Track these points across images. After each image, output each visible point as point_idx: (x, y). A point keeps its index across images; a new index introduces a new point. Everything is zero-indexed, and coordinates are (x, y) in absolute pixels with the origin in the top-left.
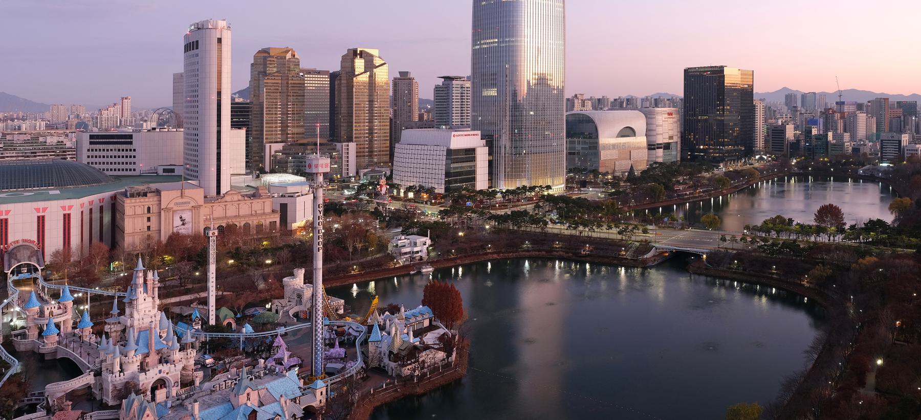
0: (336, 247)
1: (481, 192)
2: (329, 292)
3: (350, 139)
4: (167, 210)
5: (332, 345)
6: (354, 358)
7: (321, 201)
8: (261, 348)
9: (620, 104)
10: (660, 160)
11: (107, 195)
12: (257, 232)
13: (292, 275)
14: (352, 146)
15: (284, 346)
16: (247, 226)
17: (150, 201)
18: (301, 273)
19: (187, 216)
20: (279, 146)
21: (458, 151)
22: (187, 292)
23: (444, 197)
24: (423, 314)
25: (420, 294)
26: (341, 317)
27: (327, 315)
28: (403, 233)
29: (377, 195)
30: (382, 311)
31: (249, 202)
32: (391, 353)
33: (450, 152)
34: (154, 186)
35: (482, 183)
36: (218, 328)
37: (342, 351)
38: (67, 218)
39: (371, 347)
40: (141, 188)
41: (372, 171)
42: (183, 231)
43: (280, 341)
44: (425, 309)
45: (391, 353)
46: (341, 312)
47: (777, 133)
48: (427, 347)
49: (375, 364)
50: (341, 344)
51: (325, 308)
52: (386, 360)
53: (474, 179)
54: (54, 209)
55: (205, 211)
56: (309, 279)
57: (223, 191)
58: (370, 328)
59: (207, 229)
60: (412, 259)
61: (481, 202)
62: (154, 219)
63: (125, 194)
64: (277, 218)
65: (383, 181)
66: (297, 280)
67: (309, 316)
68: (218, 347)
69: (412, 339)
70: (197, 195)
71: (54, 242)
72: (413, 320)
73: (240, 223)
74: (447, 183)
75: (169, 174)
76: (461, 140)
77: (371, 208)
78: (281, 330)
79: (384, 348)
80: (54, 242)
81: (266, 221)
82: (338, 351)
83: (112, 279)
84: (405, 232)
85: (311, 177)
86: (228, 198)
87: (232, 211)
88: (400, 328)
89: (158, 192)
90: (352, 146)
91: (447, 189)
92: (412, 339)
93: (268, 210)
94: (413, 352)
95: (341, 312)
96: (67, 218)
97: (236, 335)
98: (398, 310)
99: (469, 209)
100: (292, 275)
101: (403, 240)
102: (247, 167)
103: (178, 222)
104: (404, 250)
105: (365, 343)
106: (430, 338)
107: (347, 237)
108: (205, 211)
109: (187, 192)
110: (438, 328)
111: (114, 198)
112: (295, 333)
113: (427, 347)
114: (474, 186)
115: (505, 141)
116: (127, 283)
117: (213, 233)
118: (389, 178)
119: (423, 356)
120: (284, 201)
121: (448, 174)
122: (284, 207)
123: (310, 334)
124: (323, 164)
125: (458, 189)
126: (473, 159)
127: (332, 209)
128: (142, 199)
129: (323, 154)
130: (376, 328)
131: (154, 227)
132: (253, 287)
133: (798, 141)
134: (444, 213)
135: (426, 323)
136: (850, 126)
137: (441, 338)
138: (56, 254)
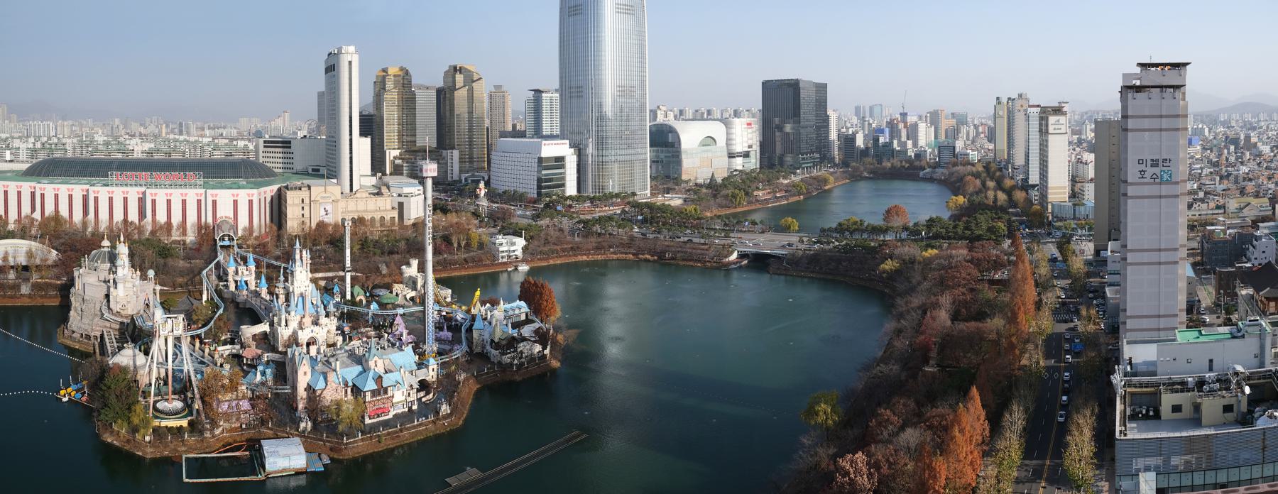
0: (444, 241)
1: (570, 198)
2: (439, 281)
3: (453, 148)
4: (316, 201)
5: (441, 329)
6: (460, 342)
7: (430, 201)
8: (382, 326)
9: (698, 117)
10: (740, 168)
11: (275, 188)
12: (381, 226)
13: (408, 264)
14: (456, 153)
15: (403, 325)
16: (373, 219)
17: (304, 193)
18: (415, 263)
19: (329, 208)
20: (397, 153)
21: (548, 159)
22: (329, 271)
23: (535, 202)
24: (521, 308)
25: (517, 290)
26: (449, 305)
27: (437, 302)
28: (500, 233)
29: (477, 196)
30: (483, 303)
31: (374, 198)
32: (492, 341)
33: (540, 160)
34: (306, 182)
35: (571, 190)
36: (353, 302)
37: (450, 335)
38: (251, 202)
39: (475, 334)
40: (298, 183)
41: (473, 176)
42: (326, 220)
43: (399, 320)
44: (523, 304)
45: (492, 341)
46: (449, 300)
47: (848, 141)
48: (524, 339)
49: (477, 350)
50: (449, 329)
51: (436, 295)
52: (488, 347)
53: (563, 185)
54: (243, 195)
55: (342, 204)
56: (422, 268)
57: (355, 189)
58: (474, 318)
59: (343, 220)
60: (509, 257)
61: (570, 206)
62: (307, 208)
63: (287, 187)
64: (395, 214)
65: (482, 185)
66: (411, 270)
67: (423, 301)
68: (351, 319)
69: (510, 331)
70: (337, 190)
71: (243, 222)
72: (511, 313)
73: (367, 217)
74: (539, 187)
75: (316, 173)
76: (550, 150)
77: (472, 208)
78: (400, 311)
79: (487, 337)
80: (243, 222)
81: (387, 218)
82: (446, 334)
83: (278, 253)
84: (504, 231)
85: (422, 181)
86: (358, 195)
87: (361, 207)
88: (501, 315)
89: (309, 187)
90: (456, 153)
91: (539, 194)
92: (510, 331)
93: (389, 207)
94: (512, 343)
95: (449, 300)
96: (251, 202)
97: (365, 310)
98: (498, 303)
99: (559, 212)
100: (408, 264)
101: (500, 239)
102: (372, 169)
103: (323, 213)
104: (501, 249)
105: (470, 330)
106: (527, 331)
107: (451, 234)
108: (342, 204)
109: (329, 188)
110: (532, 322)
111: (279, 190)
112: (412, 314)
113: (524, 339)
114: (564, 192)
115: (591, 150)
116: (288, 257)
117: (348, 224)
118: (487, 184)
119: (522, 347)
120: (401, 200)
121: (539, 180)
122: (401, 205)
123: (422, 318)
124: (431, 169)
125: (548, 195)
126: (563, 167)
127: (439, 208)
128: (298, 192)
129: (432, 159)
130: (478, 319)
131: (307, 215)
132: (378, 270)
133: (867, 148)
134: (536, 217)
135: (523, 317)
136: (913, 132)
137: (537, 332)
138: (245, 229)
